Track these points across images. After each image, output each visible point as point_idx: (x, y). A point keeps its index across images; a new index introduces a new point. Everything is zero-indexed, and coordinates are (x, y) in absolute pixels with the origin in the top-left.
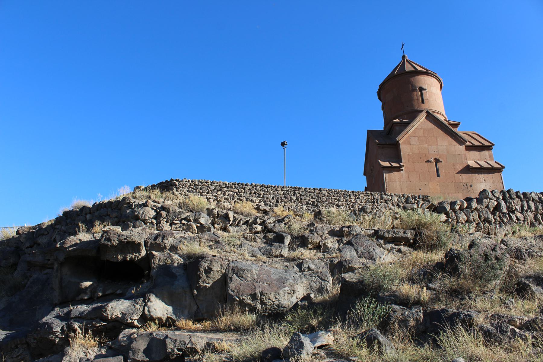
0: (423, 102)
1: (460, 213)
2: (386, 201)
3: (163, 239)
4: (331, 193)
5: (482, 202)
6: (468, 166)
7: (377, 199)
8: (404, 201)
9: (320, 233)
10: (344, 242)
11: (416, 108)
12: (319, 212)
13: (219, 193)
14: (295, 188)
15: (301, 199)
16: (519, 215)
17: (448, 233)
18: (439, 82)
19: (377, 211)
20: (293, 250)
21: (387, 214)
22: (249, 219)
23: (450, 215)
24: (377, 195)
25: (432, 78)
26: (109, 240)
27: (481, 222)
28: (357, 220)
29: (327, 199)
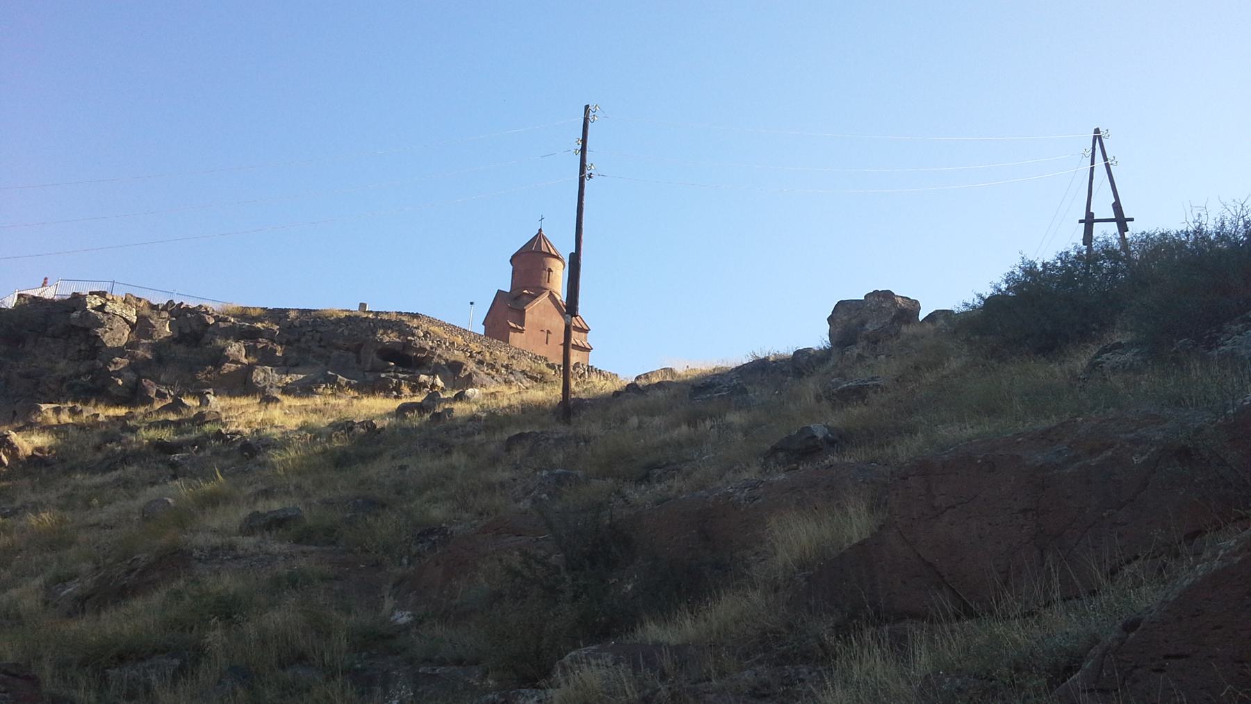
0: (548, 282)
26: (416, 345)
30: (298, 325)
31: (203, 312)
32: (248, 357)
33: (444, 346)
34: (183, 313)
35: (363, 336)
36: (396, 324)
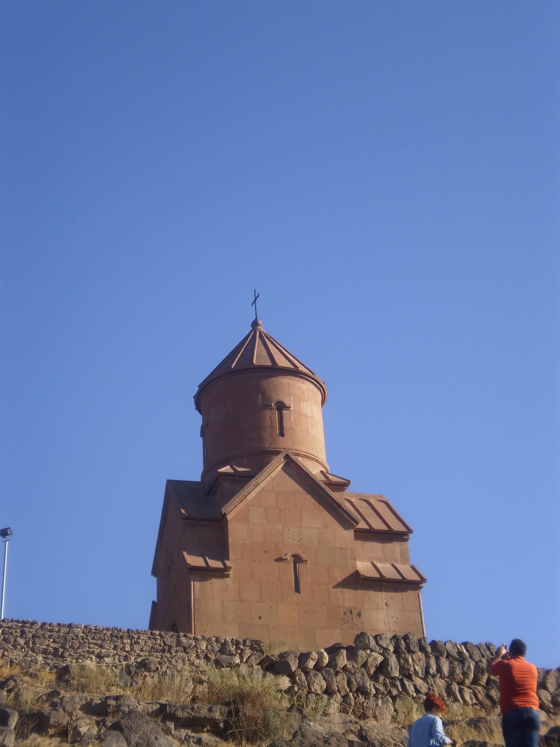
0: (282, 434)
1: (316, 675)
2: (185, 648)
4: (89, 632)
5: (357, 655)
6: (357, 572)
7: (169, 646)
8: (218, 649)
9: (69, 708)
10: (109, 724)
11: (267, 445)
12: (66, 669)
14: (23, 622)
15: (34, 643)
16: (419, 682)
17: (283, 714)
18: (319, 388)
19: (167, 668)
20: (23, 738)
21: (186, 674)
23: (297, 677)
24: (171, 637)
25: (306, 382)
27: (351, 694)
28: (131, 685)
29: (80, 643)
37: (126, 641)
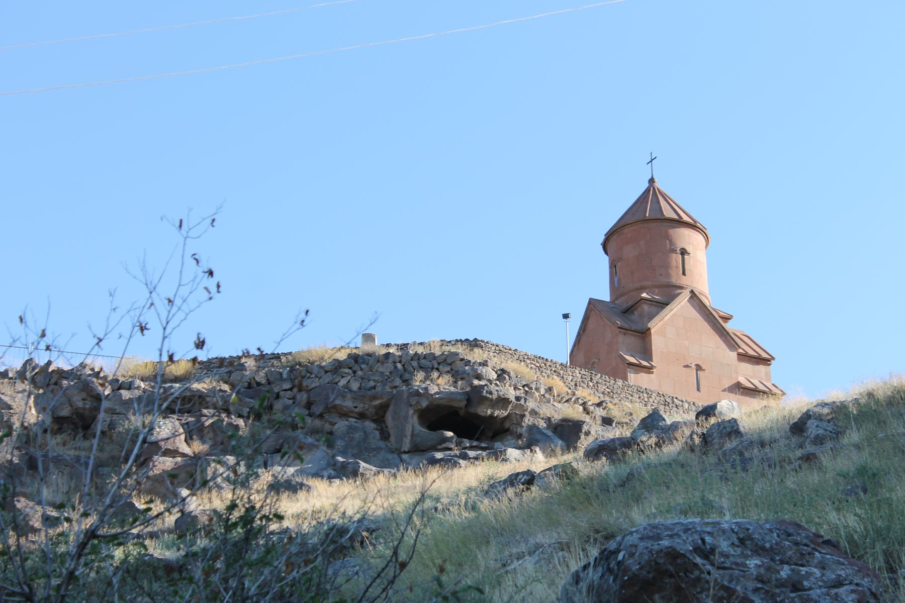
0: (684, 274)
3: (525, 402)
11: (674, 281)
13: (523, 363)
15: (597, 386)
22: (571, 399)
26: (491, 393)
30: (264, 381)
31: (90, 375)
32: (190, 442)
33: (537, 394)
34: (53, 381)
35: (388, 389)
36: (445, 360)
37: (645, 395)
